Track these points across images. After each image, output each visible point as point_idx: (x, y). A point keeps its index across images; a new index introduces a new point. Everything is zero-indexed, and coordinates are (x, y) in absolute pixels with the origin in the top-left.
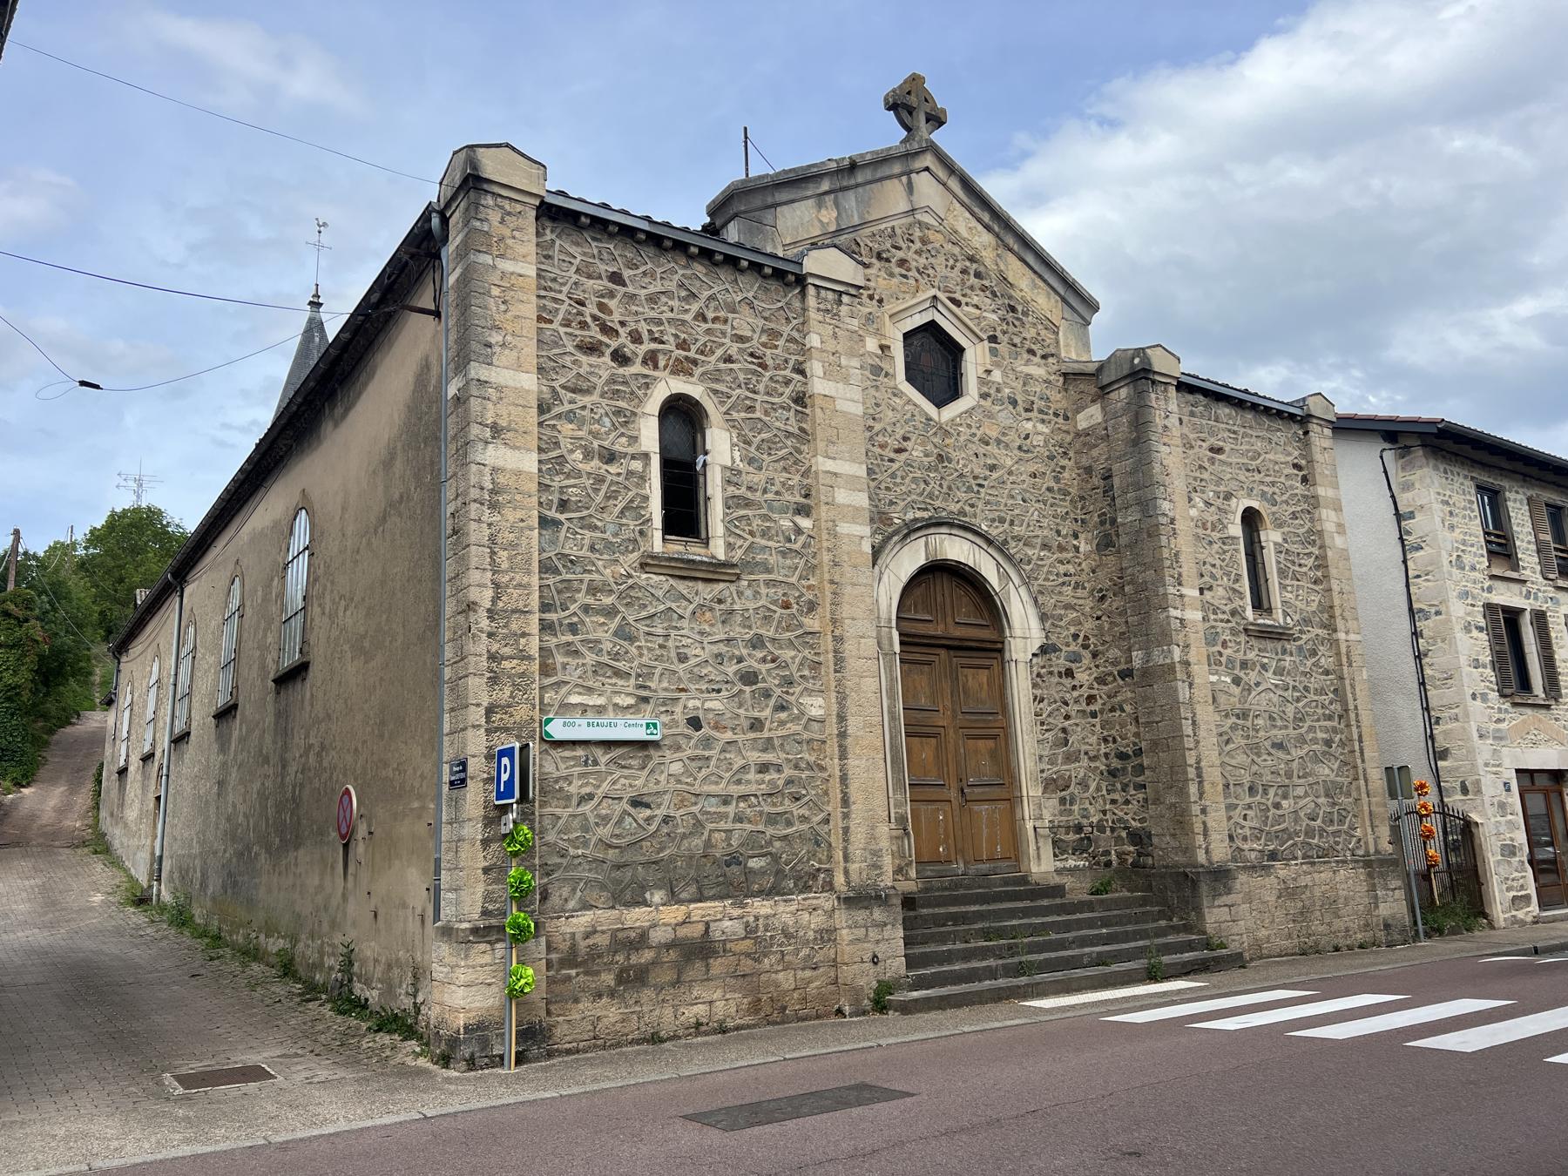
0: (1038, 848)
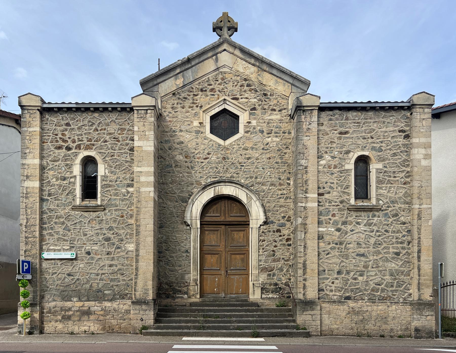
0: (254, 291)
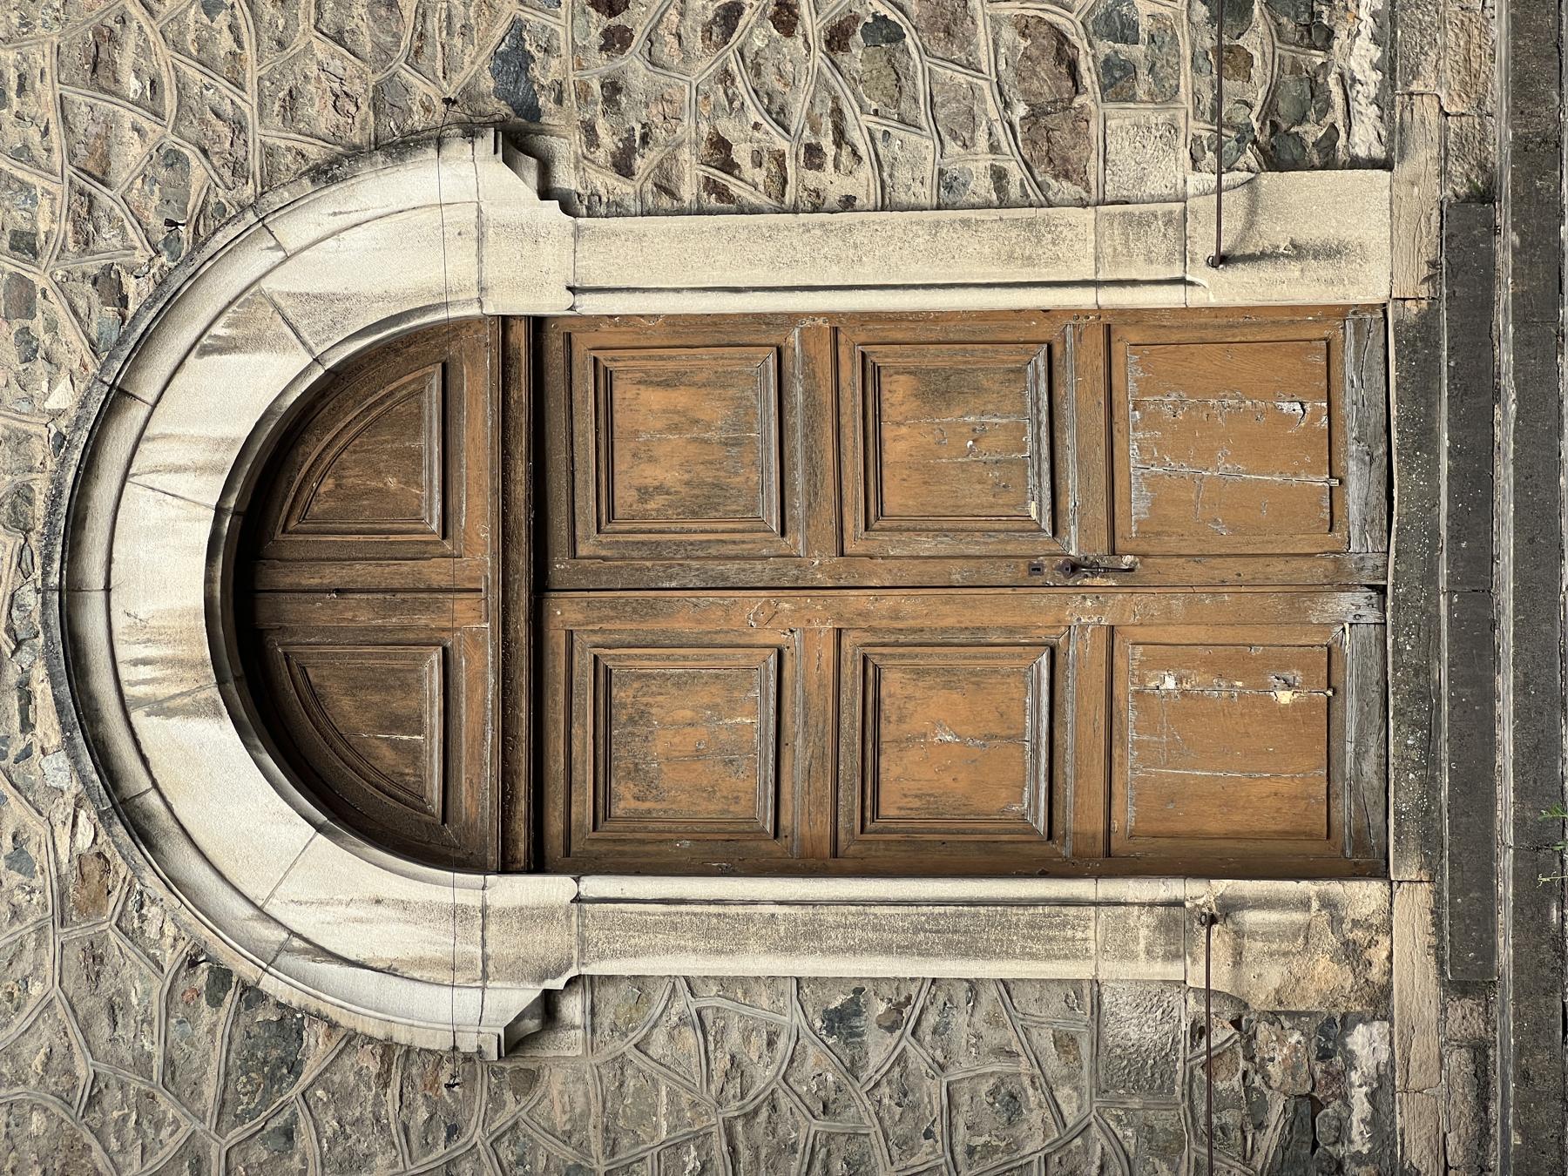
0: (1298, 251)
